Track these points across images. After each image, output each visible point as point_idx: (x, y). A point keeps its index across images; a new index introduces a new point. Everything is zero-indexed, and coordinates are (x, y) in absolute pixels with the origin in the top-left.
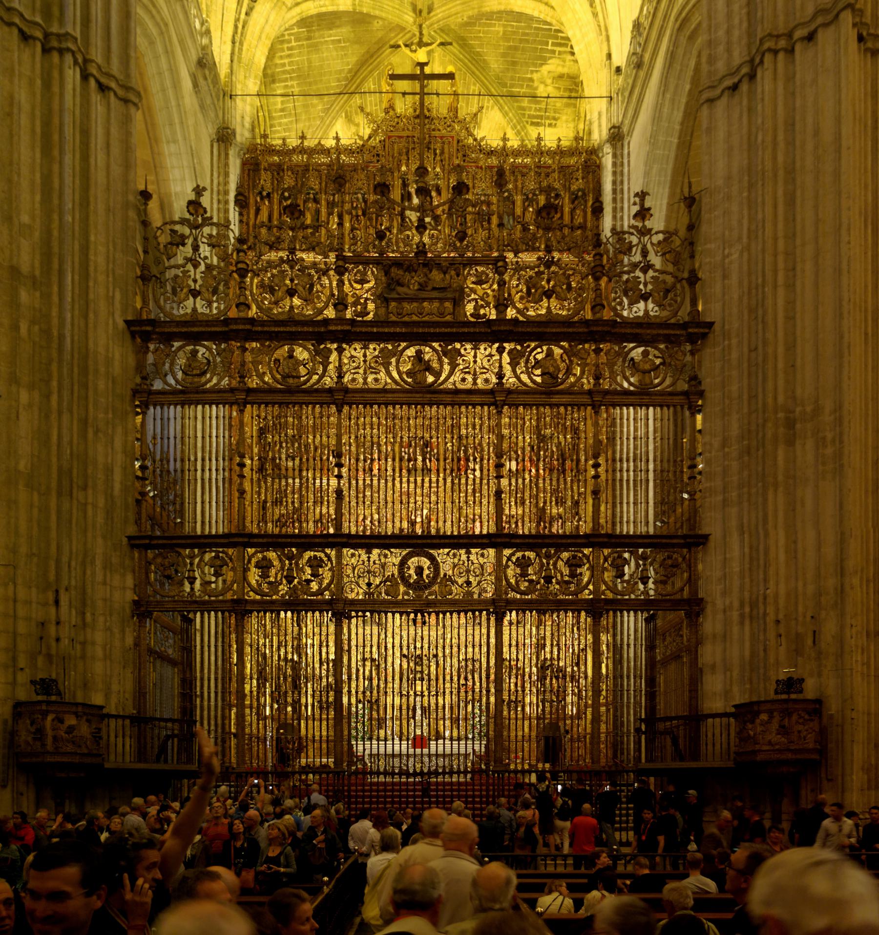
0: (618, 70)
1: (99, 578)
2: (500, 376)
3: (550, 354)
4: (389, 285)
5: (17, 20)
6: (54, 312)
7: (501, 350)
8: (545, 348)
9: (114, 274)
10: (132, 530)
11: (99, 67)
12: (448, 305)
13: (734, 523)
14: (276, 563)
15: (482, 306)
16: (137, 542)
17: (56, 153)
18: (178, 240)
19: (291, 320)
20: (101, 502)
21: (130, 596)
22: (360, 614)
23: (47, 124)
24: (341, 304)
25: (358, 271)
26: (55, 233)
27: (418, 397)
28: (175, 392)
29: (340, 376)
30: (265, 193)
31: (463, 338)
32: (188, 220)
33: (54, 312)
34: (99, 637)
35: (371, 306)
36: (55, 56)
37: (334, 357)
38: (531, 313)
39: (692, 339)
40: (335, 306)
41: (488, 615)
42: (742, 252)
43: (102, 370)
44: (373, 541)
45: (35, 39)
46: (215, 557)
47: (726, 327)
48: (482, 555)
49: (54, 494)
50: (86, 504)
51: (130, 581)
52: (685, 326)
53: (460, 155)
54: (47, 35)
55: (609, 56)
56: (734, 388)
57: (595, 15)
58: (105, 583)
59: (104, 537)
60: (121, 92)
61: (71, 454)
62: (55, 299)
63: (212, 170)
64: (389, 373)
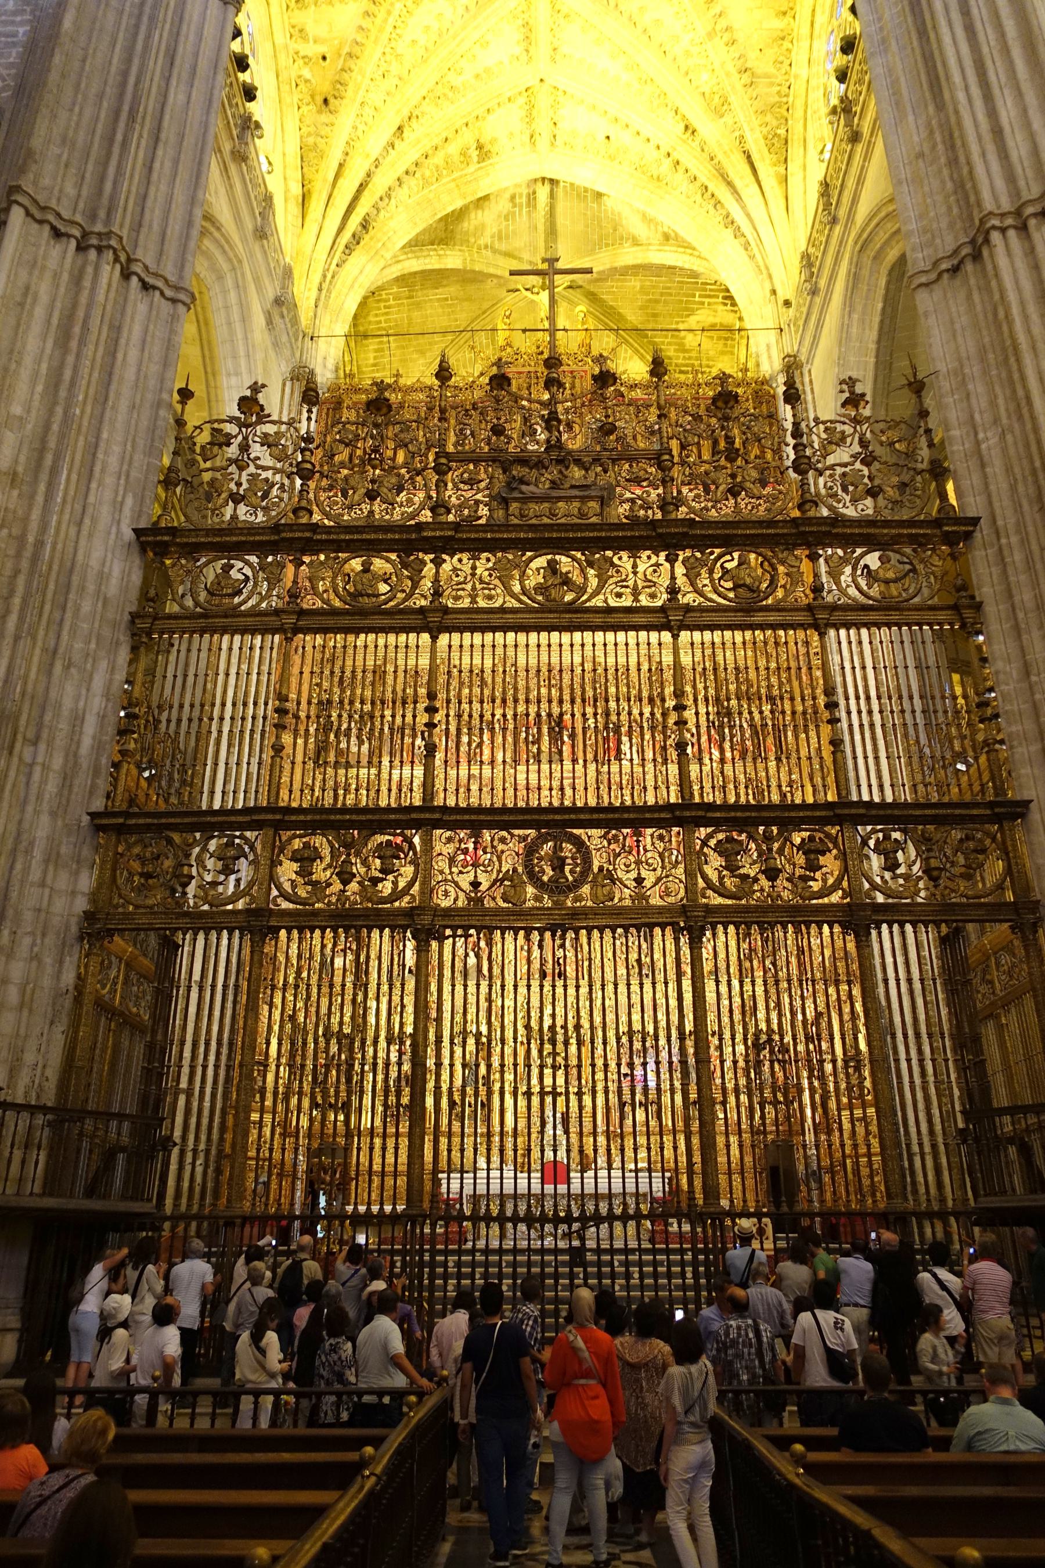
0: (787, 303)
1: (35, 875)
2: (673, 591)
4: (508, 484)
5: (51, 218)
6: (36, 515)
8: (736, 555)
9: (128, 476)
10: (98, 804)
11: (146, 267)
12: (594, 505)
16: (105, 821)
17: (74, 344)
18: (222, 440)
19: (370, 526)
20: (57, 763)
21: (81, 904)
23: (69, 318)
24: (439, 507)
26: (55, 427)
27: (551, 618)
28: (193, 616)
31: (618, 545)
32: (237, 419)
33: (36, 515)
35: (484, 511)
36: (93, 254)
37: (429, 569)
39: (950, 540)
40: (432, 510)
42: (1003, 436)
43: (91, 587)
44: (482, 817)
45: (69, 236)
46: (227, 845)
47: (1000, 523)
48: (661, 838)
50: (31, 765)
51: (86, 882)
52: (937, 523)
54: (85, 234)
55: (774, 292)
57: (752, 257)
59: (53, 814)
60: (169, 293)
61: (23, 693)
62: (40, 499)
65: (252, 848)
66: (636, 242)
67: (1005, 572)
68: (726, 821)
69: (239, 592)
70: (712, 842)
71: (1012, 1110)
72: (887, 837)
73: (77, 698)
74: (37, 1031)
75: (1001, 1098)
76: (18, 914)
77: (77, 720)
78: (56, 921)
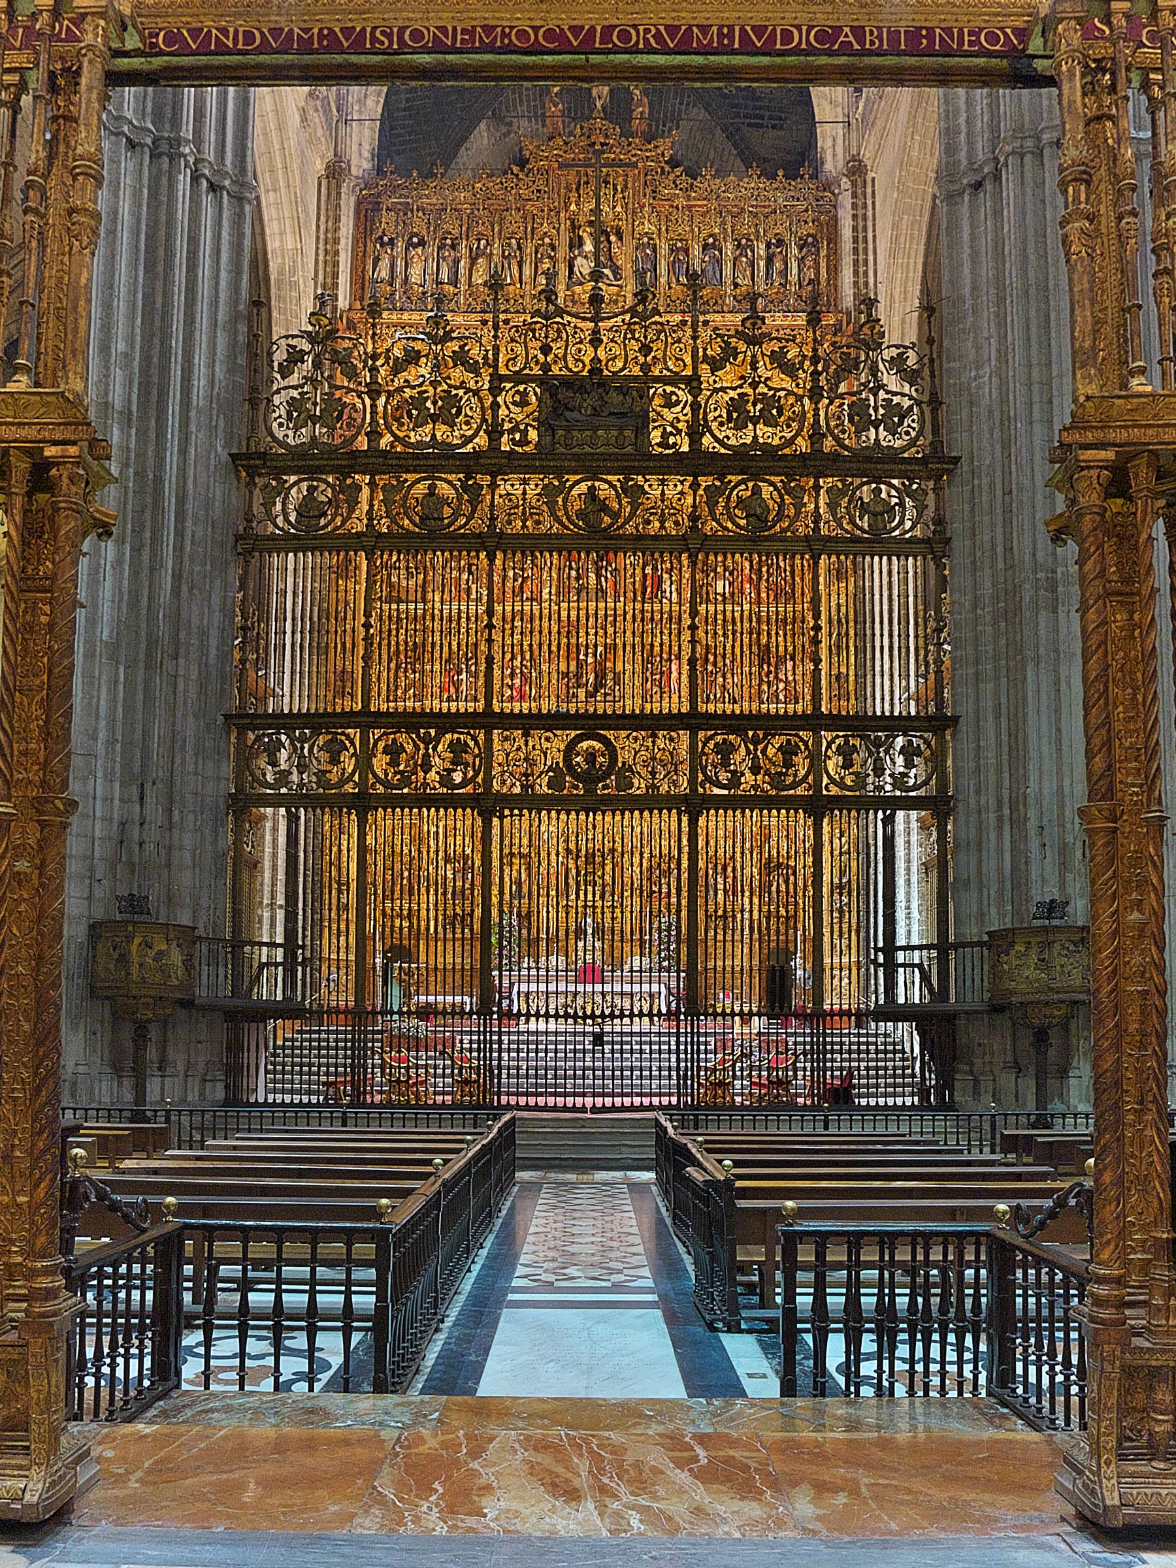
3: (757, 491)
4: (555, 409)
7: (695, 486)
8: (750, 484)
13: (988, 704)
14: (409, 748)
15: (671, 433)
18: (297, 356)
22: (516, 812)
25: (518, 392)
29: (493, 519)
30: (386, 239)
32: (309, 333)
34: (188, 840)
35: (533, 435)
38: (732, 442)
41: (679, 815)
49: (142, 665)
53: (648, 191)
58: (196, 774)
63: (319, 214)
64: (553, 513)
65: (353, 743)
67: (973, 511)
68: (723, 727)
69: (325, 514)
70: (711, 745)
71: (909, 948)
72: (847, 742)
73: (202, 615)
74: (207, 883)
75: (901, 941)
76: (183, 797)
77: (204, 634)
78: (208, 800)
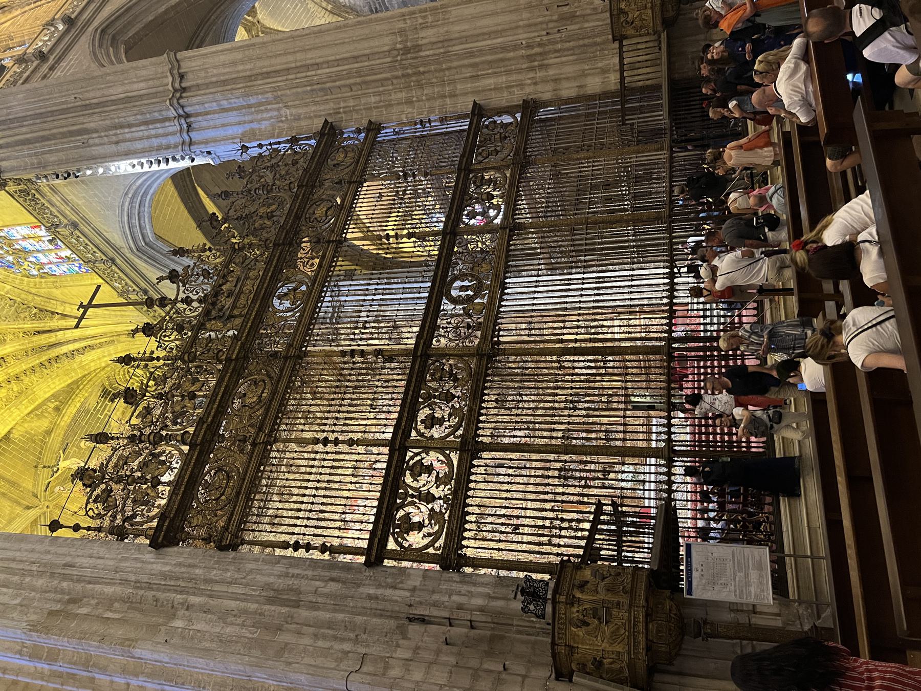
56: (373, 99)
66: (49, 432)
